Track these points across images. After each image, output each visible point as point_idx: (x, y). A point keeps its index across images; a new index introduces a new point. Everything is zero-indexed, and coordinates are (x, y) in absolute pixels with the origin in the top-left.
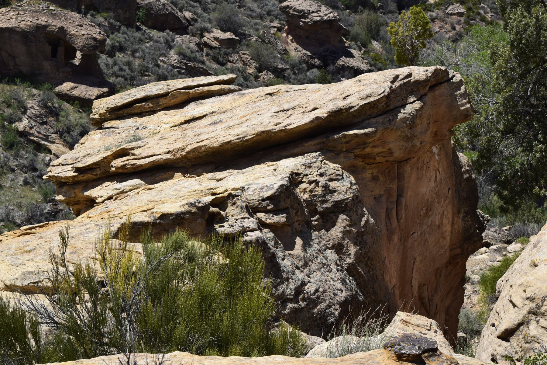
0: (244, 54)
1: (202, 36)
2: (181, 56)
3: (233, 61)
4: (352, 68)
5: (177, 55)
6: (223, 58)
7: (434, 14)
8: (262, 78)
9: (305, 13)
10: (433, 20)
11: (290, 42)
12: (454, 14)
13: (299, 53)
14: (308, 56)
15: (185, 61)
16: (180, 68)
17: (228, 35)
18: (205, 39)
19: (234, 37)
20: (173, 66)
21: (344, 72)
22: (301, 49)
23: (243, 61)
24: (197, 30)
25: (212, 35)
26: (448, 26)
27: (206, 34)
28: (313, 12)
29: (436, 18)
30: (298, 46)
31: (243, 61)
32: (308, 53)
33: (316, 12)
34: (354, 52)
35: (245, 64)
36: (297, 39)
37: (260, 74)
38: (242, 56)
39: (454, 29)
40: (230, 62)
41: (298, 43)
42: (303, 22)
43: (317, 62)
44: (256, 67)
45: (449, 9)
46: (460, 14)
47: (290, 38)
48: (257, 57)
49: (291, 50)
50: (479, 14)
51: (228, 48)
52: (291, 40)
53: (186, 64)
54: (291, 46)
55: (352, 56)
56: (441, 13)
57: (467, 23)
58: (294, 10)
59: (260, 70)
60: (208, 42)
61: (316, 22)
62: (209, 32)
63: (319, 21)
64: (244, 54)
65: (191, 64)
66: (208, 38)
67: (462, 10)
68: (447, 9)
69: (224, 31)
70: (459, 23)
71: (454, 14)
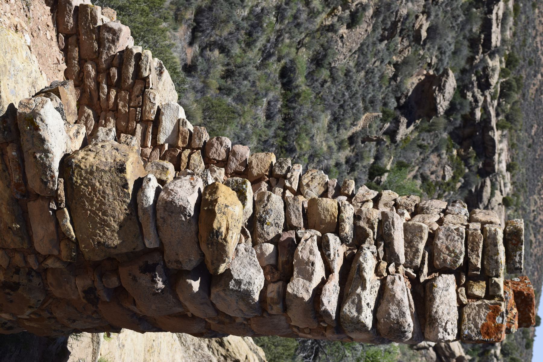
0: (409, 51)
1: (423, 13)
2: (406, 17)
3: (403, 42)
4: (398, 129)
5: (408, 13)
6: (405, 34)
7: (444, 156)
8: (389, 67)
9: (443, 90)
10: (439, 156)
11: (419, 78)
12: (444, 172)
13: (410, 86)
14: (407, 93)
15: (402, 20)
16: (396, 16)
17: (424, 34)
18: (421, 16)
19: (423, 39)
20: (398, 11)
21: (394, 123)
22: (413, 87)
23: (403, 51)
24: (429, 9)
25: (424, 22)
26: (434, 168)
27: (425, 17)
28: (443, 96)
29: (441, 158)
30: (415, 85)
31: (403, 51)
32: (410, 94)
33: (444, 98)
34: (412, 128)
35: (400, 52)
36: (421, 86)
37: (392, 66)
38: (407, 50)
39: (432, 173)
40: (402, 39)
41: (418, 84)
42: (436, 88)
43: (403, 101)
44: (397, 62)
45: (449, 168)
46: (444, 177)
47: (423, 78)
48: (406, 62)
49: (412, 79)
50: (444, 192)
51: (413, 37)
52: (420, 79)
53: (399, 21)
54: (415, 78)
55: (408, 126)
56: (444, 161)
57: (437, 183)
58: (445, 81)
59: (396, 65)
60: (419, 20)
61: (435, 99)
62: (427, 19)
63: (436, 102)
64: (409, 51)
65: (399, 24)
66: (422, 18)
67: (447, 179)
68: (449, 165)
69: (428, 31)
70: (437, 177)
71: (444, 172)
